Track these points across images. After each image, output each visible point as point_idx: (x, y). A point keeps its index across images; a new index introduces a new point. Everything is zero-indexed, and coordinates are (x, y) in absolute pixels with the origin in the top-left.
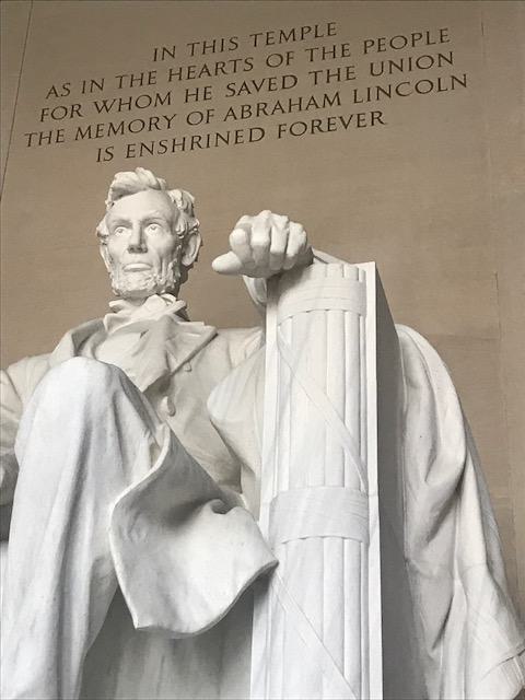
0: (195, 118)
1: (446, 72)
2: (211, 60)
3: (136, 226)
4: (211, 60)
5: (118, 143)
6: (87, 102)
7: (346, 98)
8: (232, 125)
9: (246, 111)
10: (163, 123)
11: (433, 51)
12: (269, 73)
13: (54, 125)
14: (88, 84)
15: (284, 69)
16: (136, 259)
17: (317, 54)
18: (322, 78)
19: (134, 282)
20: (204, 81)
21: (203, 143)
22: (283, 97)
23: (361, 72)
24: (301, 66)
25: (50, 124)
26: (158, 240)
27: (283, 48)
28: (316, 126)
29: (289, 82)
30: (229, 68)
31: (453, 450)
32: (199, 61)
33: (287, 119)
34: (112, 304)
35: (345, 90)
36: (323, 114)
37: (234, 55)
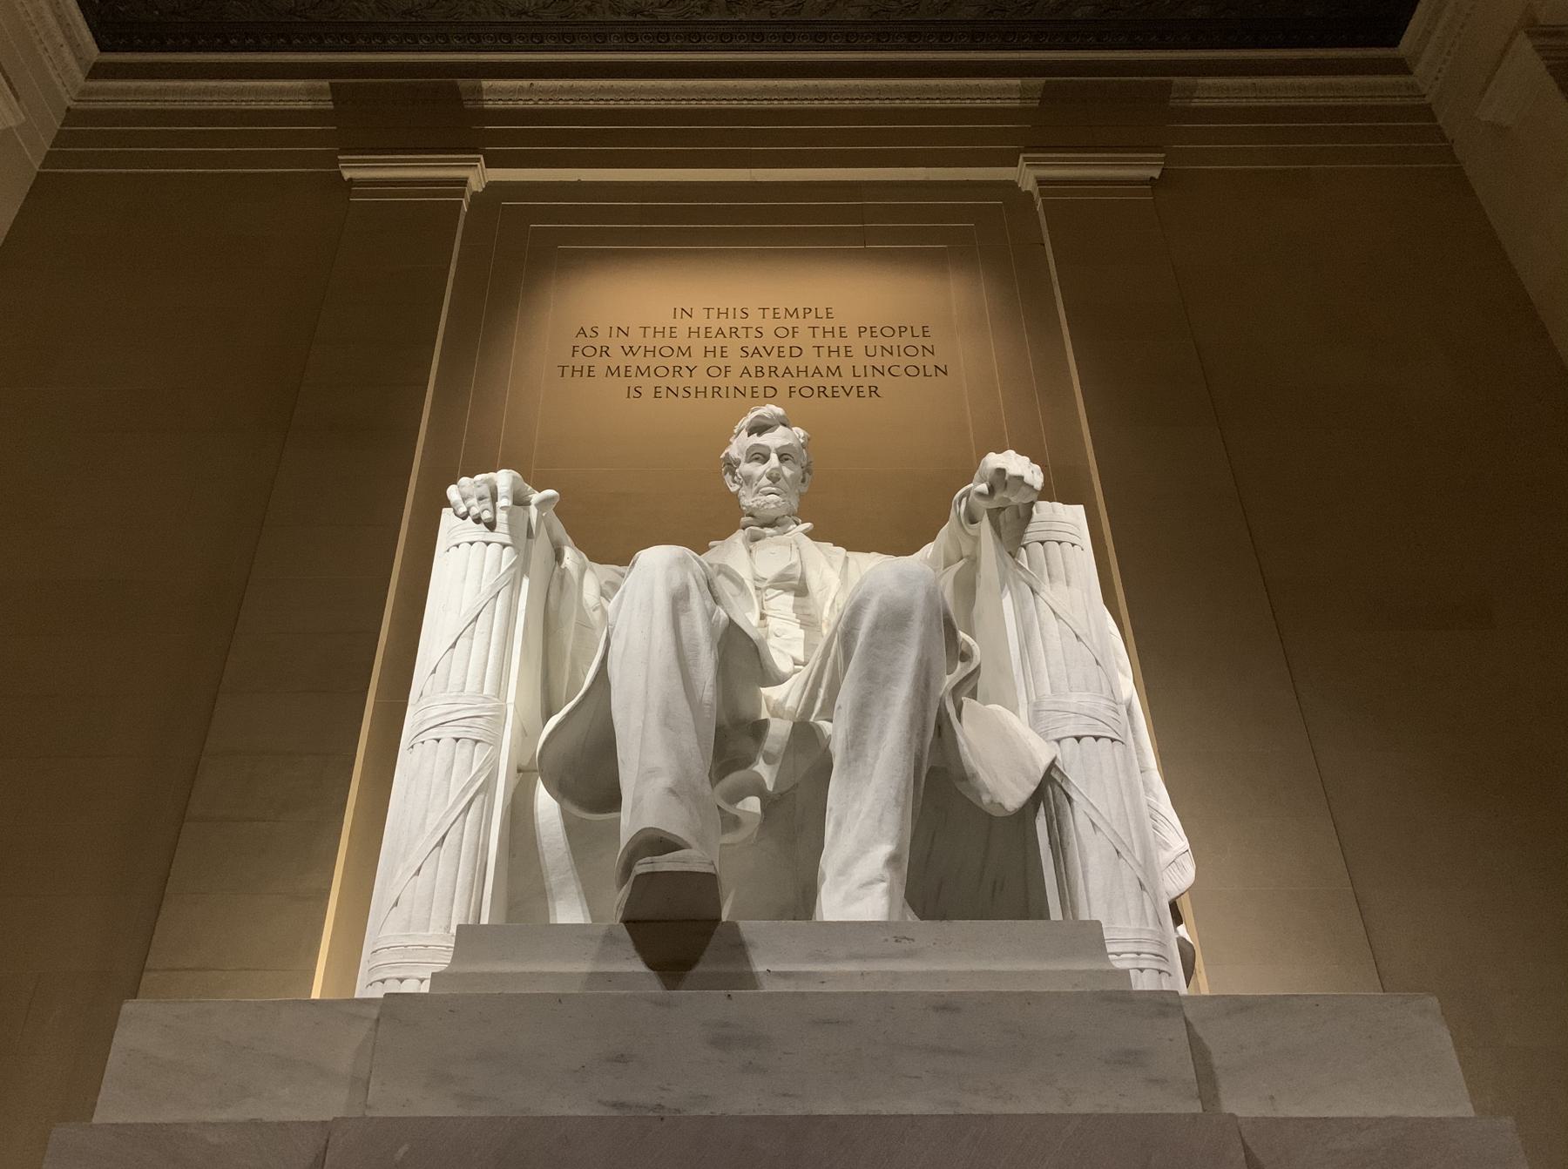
0: (714, 372)
1: (929, 361)
2: (726, 324)
3: (774, 457)
5: (647, 384)
8: (747, 382)
9: (759, 371)
10: (685, 372)
11: (919, 342)
12: (778, 342)
14: (615, 330)
15: (788, 342)
17: (819, 332)
18: (824, 351)
19: (771, 502)
21: (723, 392)
23: (858, 351)
27: (790, 322)
29: (796, 352)
30: (741, 333)
32: (715, 324)
33: (799, 382)
34: (744, 520)
35: (846, 365)
37: (746, 323)
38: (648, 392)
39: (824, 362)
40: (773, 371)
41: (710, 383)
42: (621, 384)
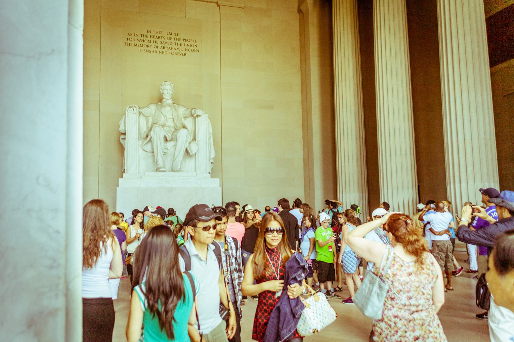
2: (158, 35)
4: (158, 35)
5: (142, 49)
6: (136, 38)
7: (180, 49)
8: (161, 50)
9: (164, 48)
11: (194, 44)
12: (168, 41)
13: (130, 42)
15: (169, 41)
16: (168, 95)
19: (168, 98)
20: (156, 40)
22: (170, 46)
23: (183, 45)
24: (173, 41)
25: (129, 42)
26: (171, 92)
28: (175, 54)
31: (211, 131)
32: (156, 35)
33: (172, 51)
35: (180, 47)
36: (177, 51)
37: (161, 35)
38: (143, 51)
39: (176, 47)
40: (167, 48)
41: (155, 49)
42: (137, 48)
